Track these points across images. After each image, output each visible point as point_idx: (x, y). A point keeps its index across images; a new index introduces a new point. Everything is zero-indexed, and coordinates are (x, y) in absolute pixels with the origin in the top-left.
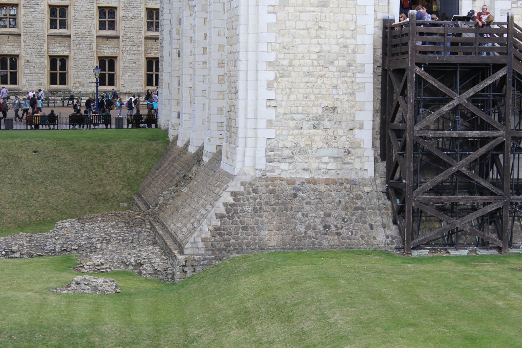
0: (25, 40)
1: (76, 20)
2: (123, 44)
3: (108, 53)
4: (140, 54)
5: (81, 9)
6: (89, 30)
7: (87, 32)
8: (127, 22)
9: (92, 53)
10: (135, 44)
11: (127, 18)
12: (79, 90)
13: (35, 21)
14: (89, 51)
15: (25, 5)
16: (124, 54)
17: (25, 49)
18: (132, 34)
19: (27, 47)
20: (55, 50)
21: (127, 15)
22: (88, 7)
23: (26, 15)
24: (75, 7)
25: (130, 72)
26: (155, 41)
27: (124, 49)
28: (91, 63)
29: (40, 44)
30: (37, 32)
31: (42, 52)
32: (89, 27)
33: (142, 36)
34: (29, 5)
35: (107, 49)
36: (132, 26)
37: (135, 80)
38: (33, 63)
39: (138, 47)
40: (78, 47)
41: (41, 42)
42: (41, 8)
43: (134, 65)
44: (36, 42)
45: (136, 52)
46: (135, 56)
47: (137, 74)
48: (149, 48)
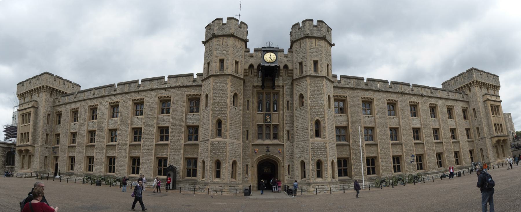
2: (143, 149)
12: (118, 176)
16: (143, 155)
26: (162, 147)
43: (148, 162)
48: (158, 151)
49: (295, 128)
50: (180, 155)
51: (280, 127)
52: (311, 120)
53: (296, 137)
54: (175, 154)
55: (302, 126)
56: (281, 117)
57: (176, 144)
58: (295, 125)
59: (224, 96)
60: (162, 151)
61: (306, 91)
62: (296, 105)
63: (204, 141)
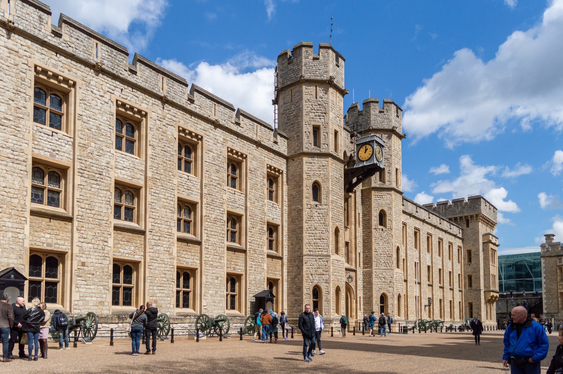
0: (79, 228)
1: (153, 210)
5: (160, 195)
6: (168, 227)
7: (166, 230)
8: (210, 224)
9: (172, 260)
10: (217, 254)
11: (210, 219)
13: (96, 200)
14: (168, 257)
15: (82, 171)
17: (80, 244)
18: (215, 240)
19: (82, 240)
20: (122, 250)
21: (210, 215)
22: (169, 195)
23: (82, 187)
24: (152, 190)
27: (207, 259)
28: (170, 275)
29: (102, 238)
30: (99, 217)
31: (106, 252)
32: (169, 223)
33: (223, 245)
34: (88, 173)
36: (214, 230)
38: (92, 268)
39: (220, 258)
40: (155, 249)
41: (105, 235)
42: (105, 181)
44: (97, 234)
49: (374, 253)
50: (263, 273)
51: (351, 247)
52: (395, 246)
53: (374, 264)
54: (256, 269)
55: (383, 252)
56: (353, 233)
57: (256, 251)
58: (373, 248)
59: (340, 193)
60: (234, 262)
61: (390, 208)
62: (375, 223)
63: (317, 256)
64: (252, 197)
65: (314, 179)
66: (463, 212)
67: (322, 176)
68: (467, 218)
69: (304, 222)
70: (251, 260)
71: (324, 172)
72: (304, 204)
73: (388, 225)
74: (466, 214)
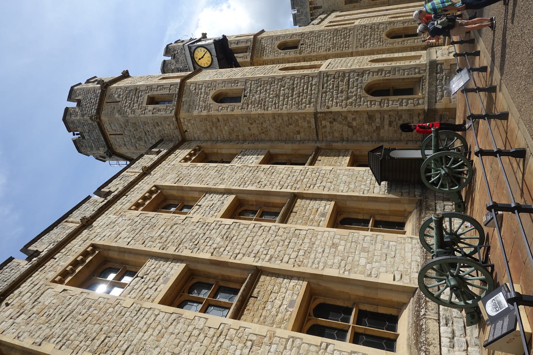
3: (291, 303)
4: (315, 235)
6: (202, 336)
7: (206, 341)
8: (228, 248)
10: (288, 241)
18: (260, 242)
21: (215, 246)
25: (357, 258)
27: (292, 261)
32: (196, 332)
35: (278, 303)
36: (242, 241)
37: (385, 251)
45: (307, 240)
46: (317, 243)
47: (365, 245)
54: (329, 180)
55: (330, 41)
64: (213, 182)
65: (211, 101)
66: (307, 13)
67: (207, 90)
68: (312, 9)
69: (266, 112)
70: (312, 187)
71: (204, 88)
72: (240, 113)
73: (297, 38)
74: (308, 10)
